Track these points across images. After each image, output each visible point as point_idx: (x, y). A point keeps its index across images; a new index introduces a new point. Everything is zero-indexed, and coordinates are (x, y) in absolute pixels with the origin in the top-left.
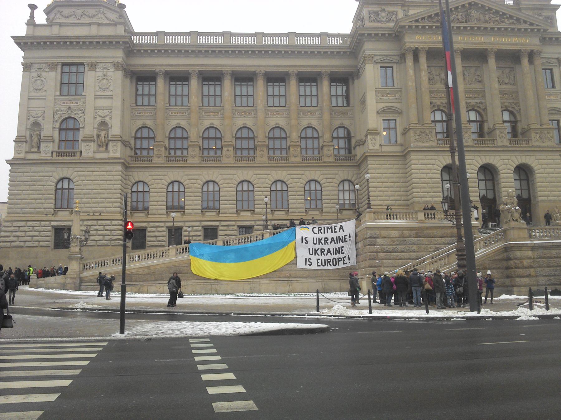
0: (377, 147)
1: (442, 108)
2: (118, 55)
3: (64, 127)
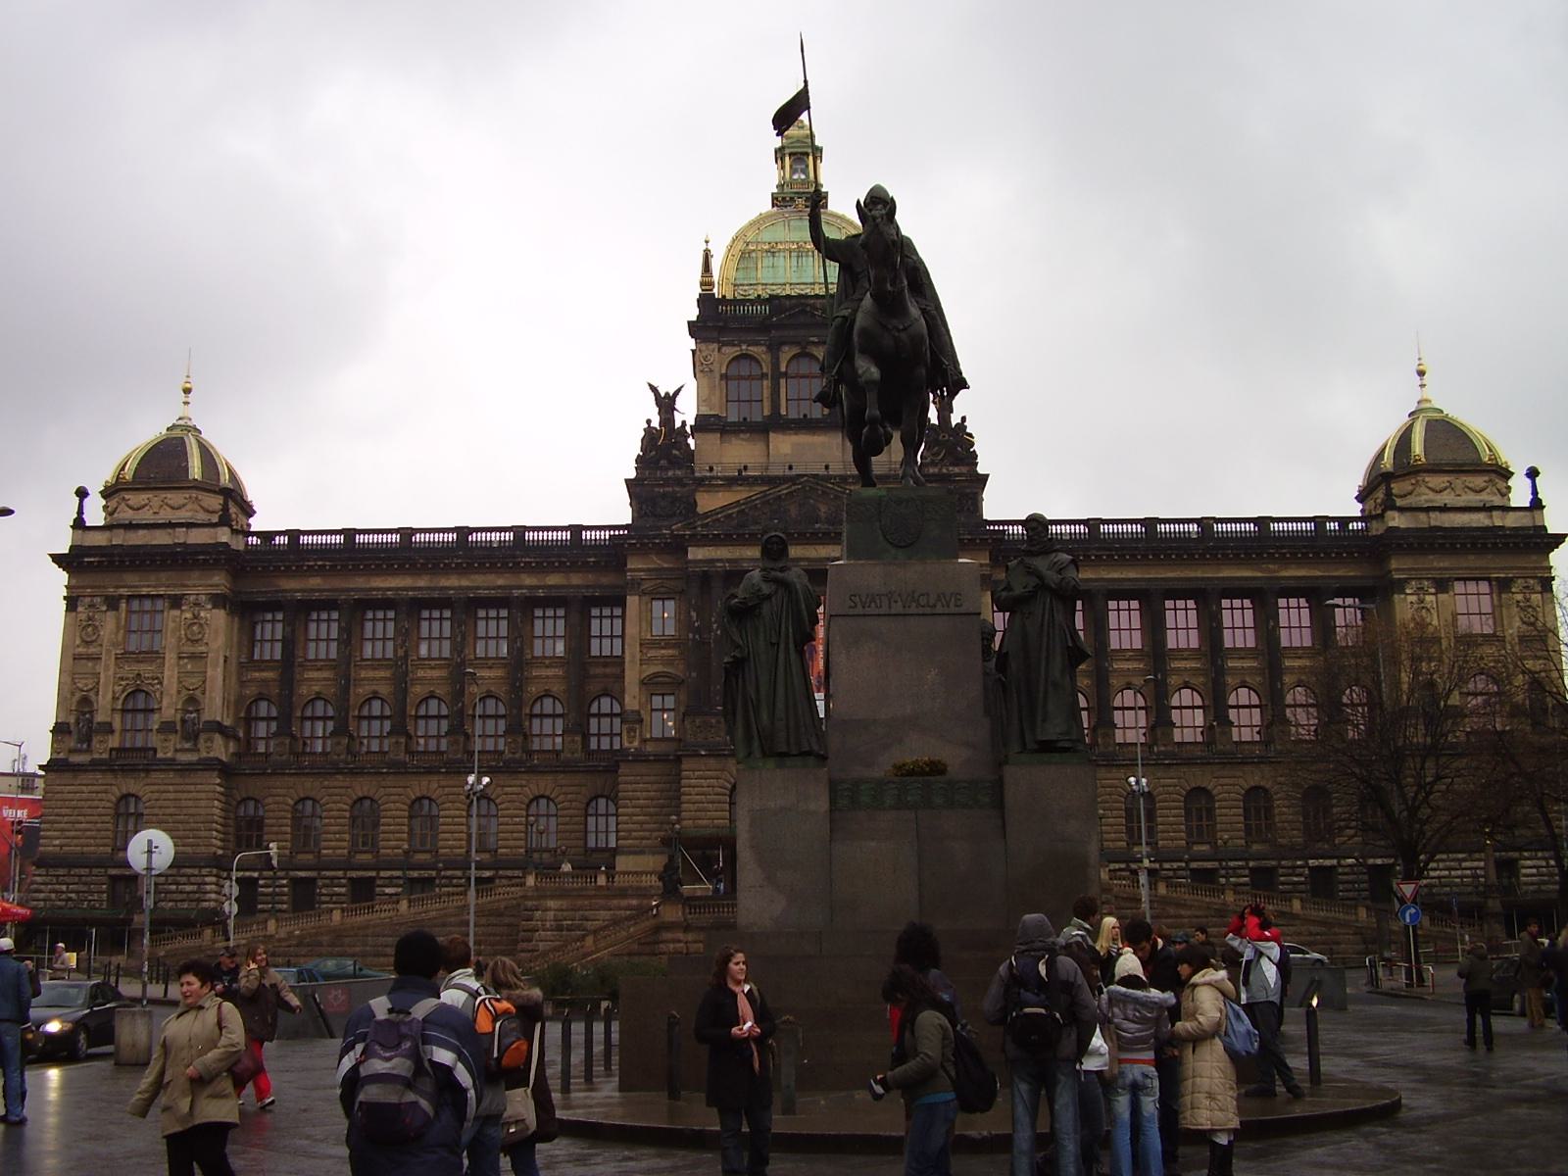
0: (636, 744)
2: (219, 581)
3: (130, 706)
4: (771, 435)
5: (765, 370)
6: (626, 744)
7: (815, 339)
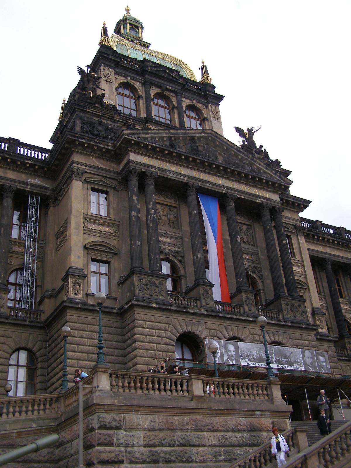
0: (80, 296)
1: (171, 258)
6: (71, 295)
7: (168, 87)
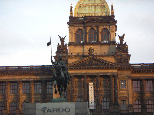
4: (85, 46)
5: (84, 32)
